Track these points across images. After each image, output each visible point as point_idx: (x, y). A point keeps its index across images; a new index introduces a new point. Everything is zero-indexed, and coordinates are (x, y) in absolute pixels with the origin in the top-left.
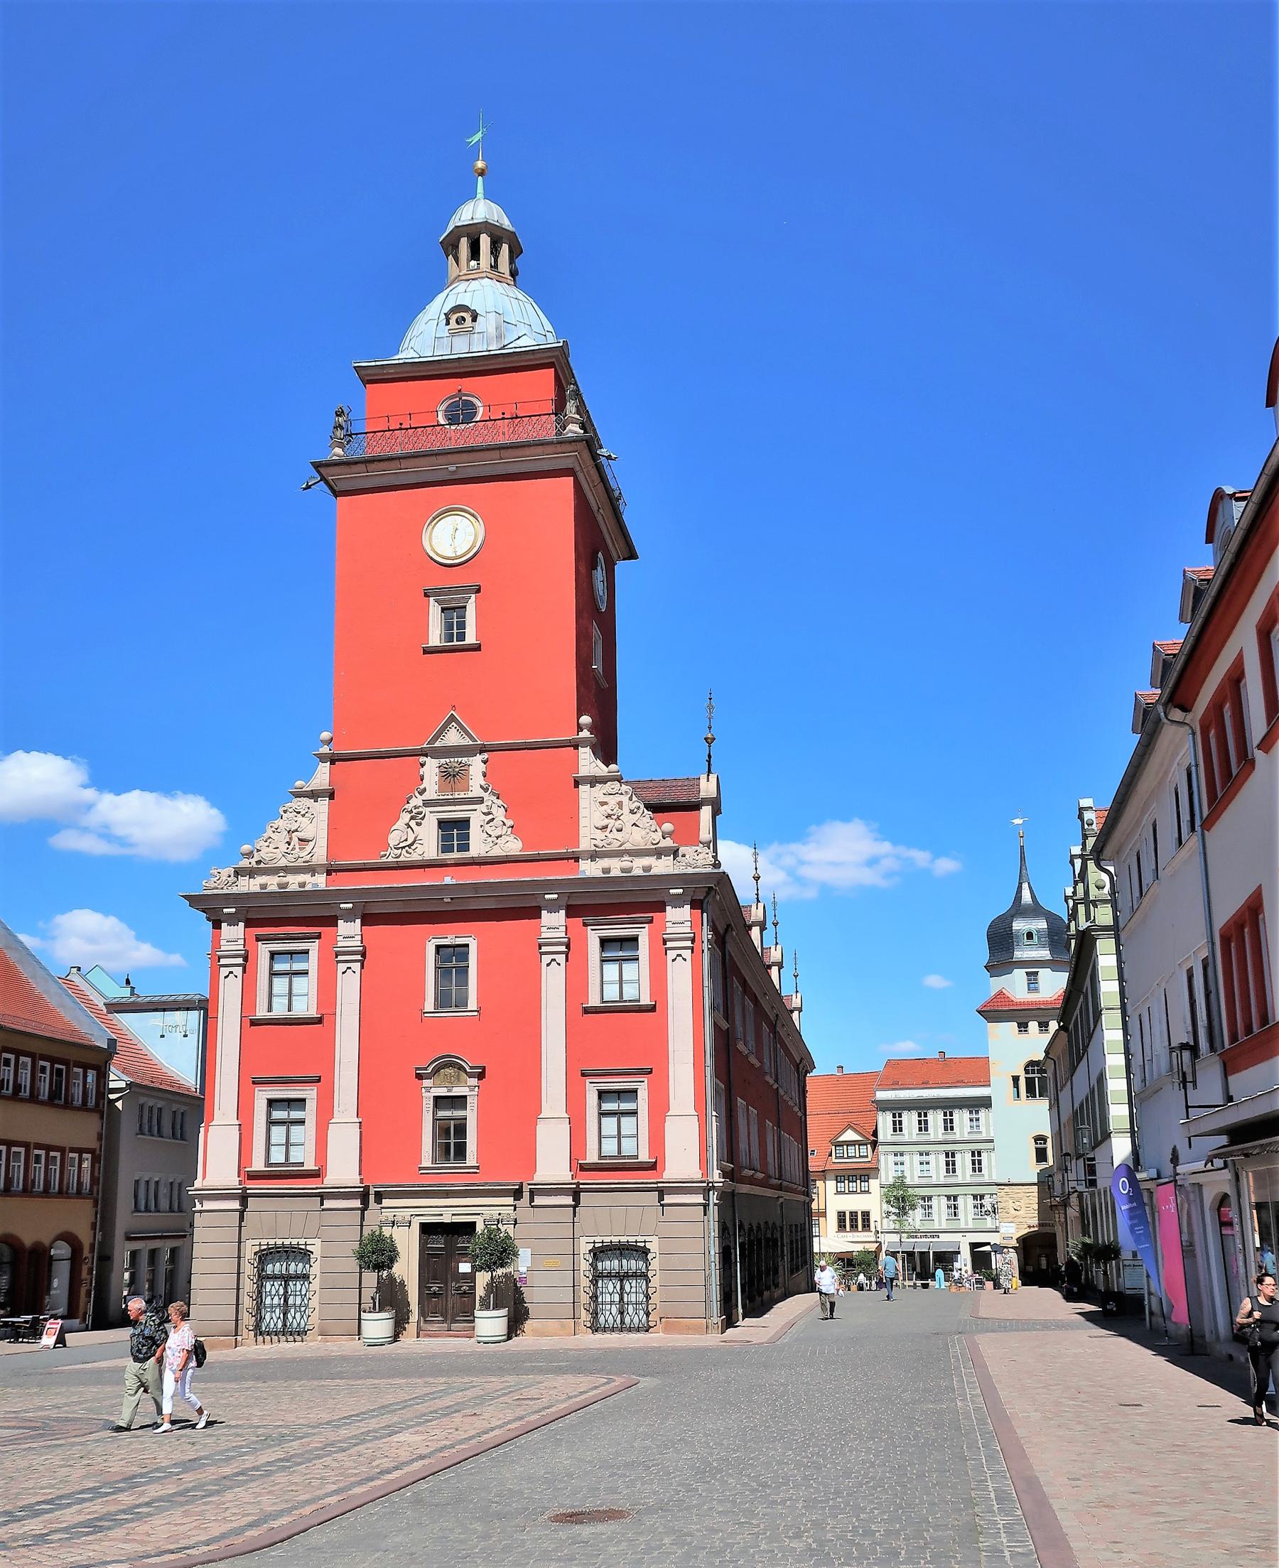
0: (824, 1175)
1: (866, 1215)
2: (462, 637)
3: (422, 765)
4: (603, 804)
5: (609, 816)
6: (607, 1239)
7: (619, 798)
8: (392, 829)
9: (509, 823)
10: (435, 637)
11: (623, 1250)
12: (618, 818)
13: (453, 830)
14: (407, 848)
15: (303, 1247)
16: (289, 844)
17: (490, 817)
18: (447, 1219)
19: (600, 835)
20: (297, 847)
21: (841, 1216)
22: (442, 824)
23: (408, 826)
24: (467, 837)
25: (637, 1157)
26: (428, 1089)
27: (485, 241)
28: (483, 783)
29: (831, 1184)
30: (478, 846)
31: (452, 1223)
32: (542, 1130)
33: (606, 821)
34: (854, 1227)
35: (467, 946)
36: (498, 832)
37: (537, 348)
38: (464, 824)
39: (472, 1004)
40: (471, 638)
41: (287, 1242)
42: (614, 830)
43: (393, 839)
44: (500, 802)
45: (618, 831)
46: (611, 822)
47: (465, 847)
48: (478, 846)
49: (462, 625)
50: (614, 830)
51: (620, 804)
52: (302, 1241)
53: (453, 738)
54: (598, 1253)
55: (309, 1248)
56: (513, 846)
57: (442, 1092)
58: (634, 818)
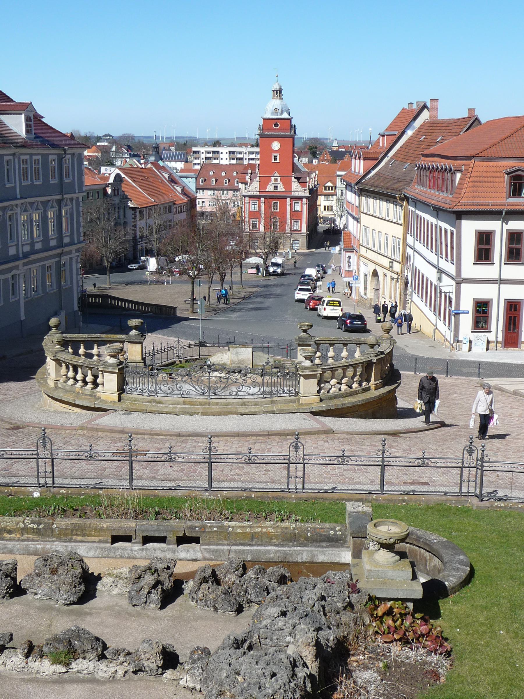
0: (321, 195)
1: (332, 207)
10: (273, 161)
11: (296, 240)
13: (276, 187)
21: (325, 206)
27: (278, 92)
29: (323, 197)
30: (278, 190)
34: (328, 210)
38: (277, 186)
39: (278, 210)
40: (278, 161)
53: (276, 175)
56: (283, 190)
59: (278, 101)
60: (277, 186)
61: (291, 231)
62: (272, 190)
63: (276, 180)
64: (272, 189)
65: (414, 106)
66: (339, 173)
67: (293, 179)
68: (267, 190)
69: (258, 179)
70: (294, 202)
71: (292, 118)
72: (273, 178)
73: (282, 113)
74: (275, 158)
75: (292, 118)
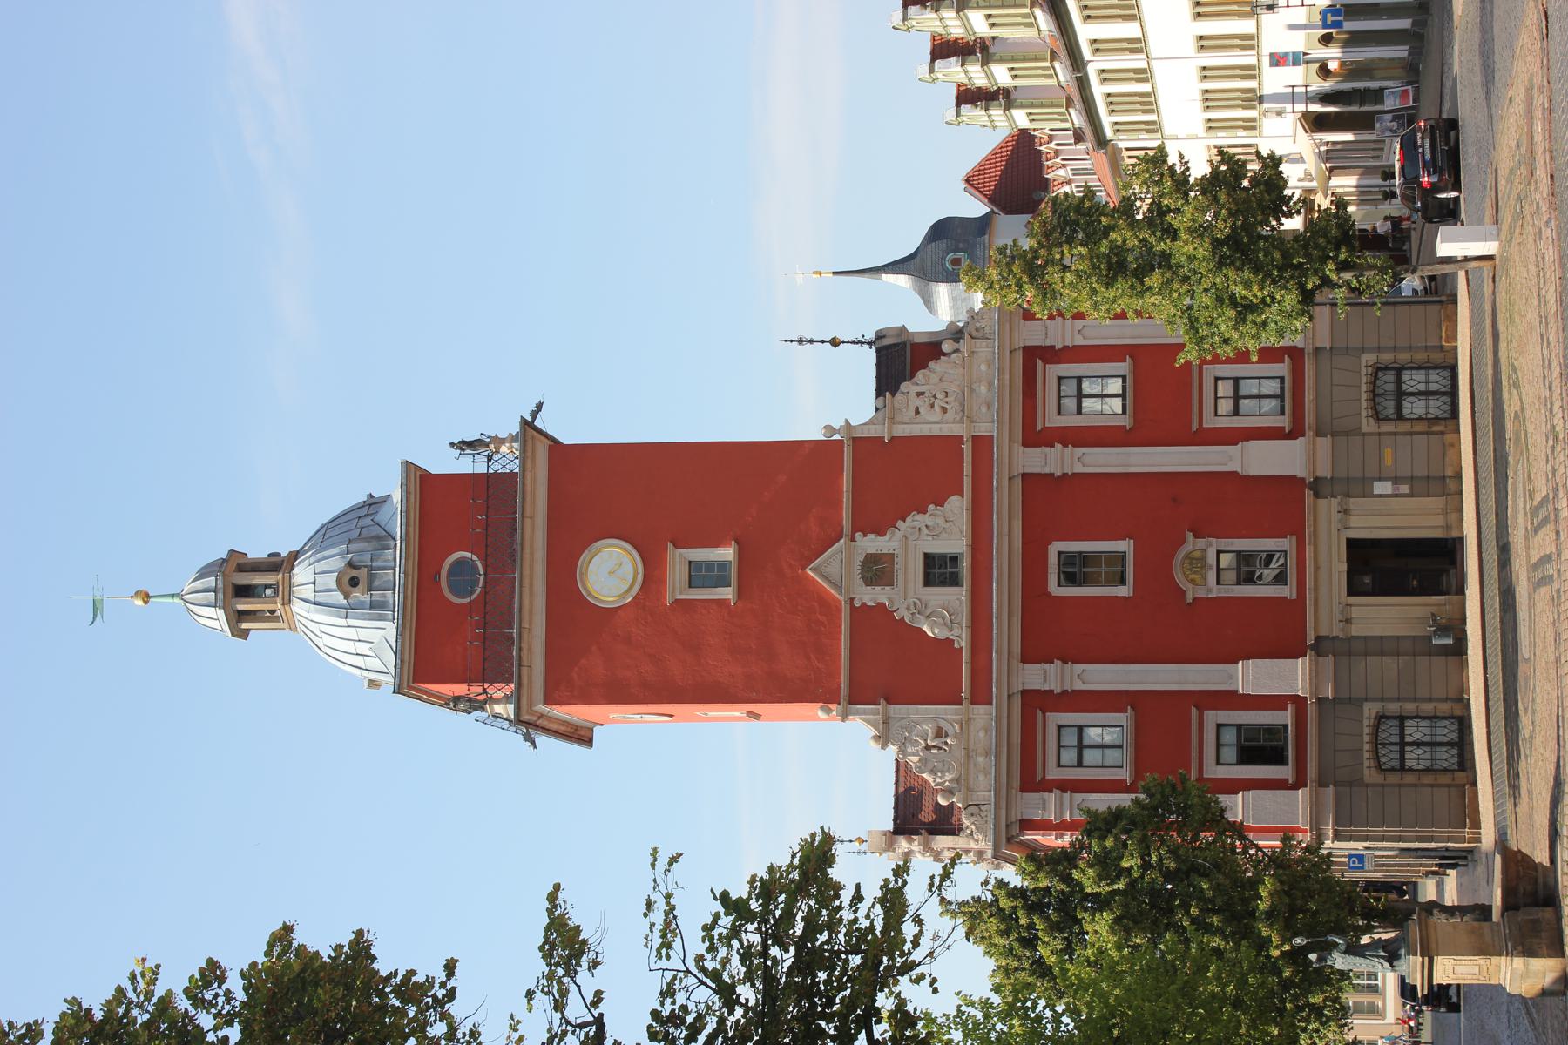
2: (724, 566)
3: (864, 604)
4: (917, 412)
5: (932, 406)
6: (1364, 404)
7: (913, 394)
8: (930, 634)
9: (931, 507)
10: (727, 593)
12: (935, 397)
13: (939, 570)
14: (953, 617)
15: (1372, 721)
16: (940, 748)
17: (925, 530)
18: (1344, 567)
19: (950, 415)
20: (943, 740)
22: (928, 582)
23: (928, 617)
24: (942, 557)
25: (1282, 379)
26: (1210, 590)
28: (887, 537)
30: (956, 543)
31: (1348, 562)
32: (1255, 470)
33: (937, 408)
35: (1060, 553)
36: (940, 521)
37: (404, 487)
38: (929, 559)
40: (727, 553)
41: (1366, 738)
42: (947, 400)
44: (909, 519)
45: (947, 397)
46: (938, 404)
47: (955, 559)
48: (956, 543)
49: (709, 566)
50: (947, 400)
51: (919, 394)
52: (1366, 722)
54: (1377, 416)
55: (1373, 715)
56: (958, 507)
57: (1212, 576)
58: (934, 378)
59: (302, 574)
60: (929, 559)
61: (1295, 433)
62: (957, 597)
63: (877, 570)
64: (957, 597)
70: (1055, 421)
72: (869, 596)
73: (383, 539)
74: (700, 575)
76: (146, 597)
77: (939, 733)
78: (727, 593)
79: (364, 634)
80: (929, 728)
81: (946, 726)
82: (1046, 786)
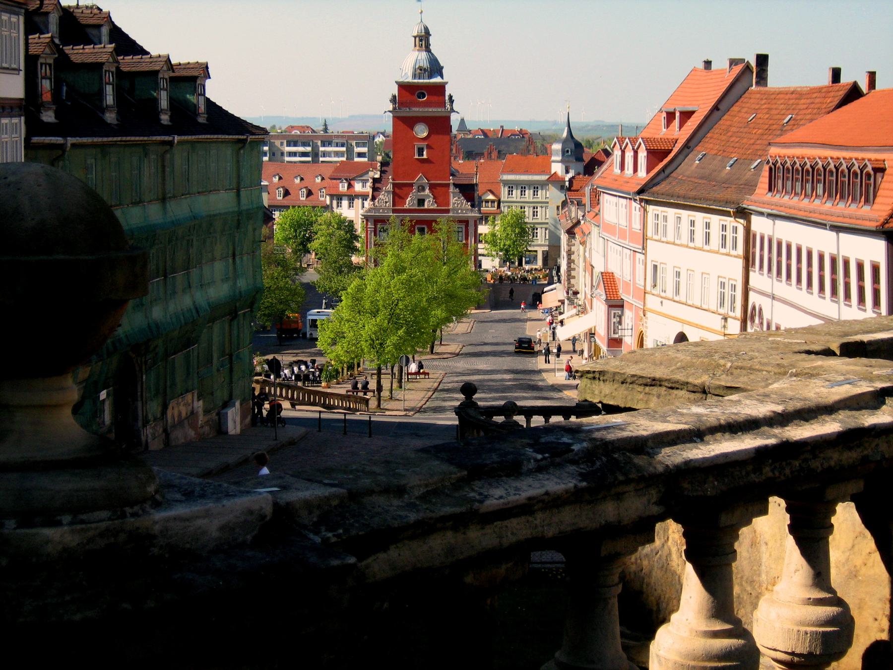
2: (423, 155)
10: (416, 157)
13: (421, 202)
30: (426, 207)
40: (425, 156)
43: (407, 203)
47: (424, 205)
49: (423, 152)
56: (435, 207)
65: (720, 64)
66: (506, 177)
67: (452, 189)
68: (407, 206)
69: (390, 187)
71: (447, 83)
75: (447, 83)
76: (421, 12)
77: (386, 202)
78: (416, 157)
79: (410, 71)
80: (387, 200)
81: (388, 204)
82: (375, 225)
